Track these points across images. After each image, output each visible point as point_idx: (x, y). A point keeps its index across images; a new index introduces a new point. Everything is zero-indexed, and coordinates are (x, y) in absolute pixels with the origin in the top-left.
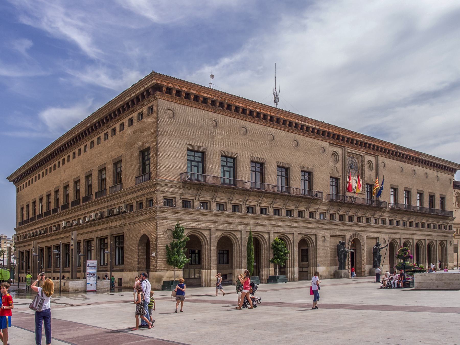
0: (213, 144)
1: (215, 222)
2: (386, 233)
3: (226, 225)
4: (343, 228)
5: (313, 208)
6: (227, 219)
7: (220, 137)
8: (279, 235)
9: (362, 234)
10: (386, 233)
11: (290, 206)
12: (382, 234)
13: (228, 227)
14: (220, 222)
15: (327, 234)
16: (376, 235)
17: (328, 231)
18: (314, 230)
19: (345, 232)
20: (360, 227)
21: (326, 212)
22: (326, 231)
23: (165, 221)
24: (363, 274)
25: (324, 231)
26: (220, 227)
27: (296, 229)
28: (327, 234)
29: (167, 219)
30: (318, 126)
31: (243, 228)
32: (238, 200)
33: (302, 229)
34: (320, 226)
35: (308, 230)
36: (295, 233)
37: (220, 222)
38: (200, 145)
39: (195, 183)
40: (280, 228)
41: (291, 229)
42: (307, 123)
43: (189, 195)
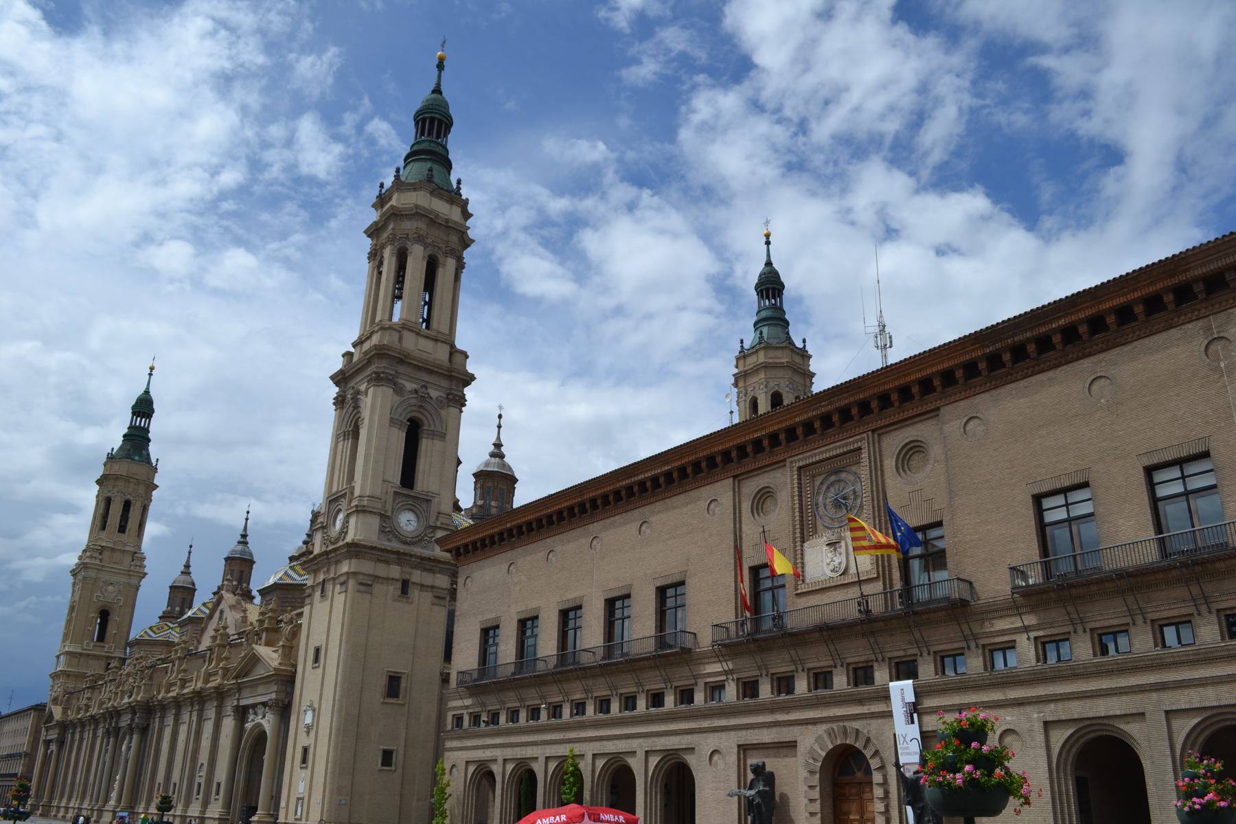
7: (518, 588)
15: (729, 743)
17: (732, 734)
19: (796, 729)
20: (860, 701)
21: (724, 678)
22: (724, 735)
26: (509, 753)
27: (641, 740)
28: (729, 743)
30: (667, 464)
32: (532, 697)
33: (655, 739)
34: (705, 724)
36: (638, 750)
40: (605, 743)
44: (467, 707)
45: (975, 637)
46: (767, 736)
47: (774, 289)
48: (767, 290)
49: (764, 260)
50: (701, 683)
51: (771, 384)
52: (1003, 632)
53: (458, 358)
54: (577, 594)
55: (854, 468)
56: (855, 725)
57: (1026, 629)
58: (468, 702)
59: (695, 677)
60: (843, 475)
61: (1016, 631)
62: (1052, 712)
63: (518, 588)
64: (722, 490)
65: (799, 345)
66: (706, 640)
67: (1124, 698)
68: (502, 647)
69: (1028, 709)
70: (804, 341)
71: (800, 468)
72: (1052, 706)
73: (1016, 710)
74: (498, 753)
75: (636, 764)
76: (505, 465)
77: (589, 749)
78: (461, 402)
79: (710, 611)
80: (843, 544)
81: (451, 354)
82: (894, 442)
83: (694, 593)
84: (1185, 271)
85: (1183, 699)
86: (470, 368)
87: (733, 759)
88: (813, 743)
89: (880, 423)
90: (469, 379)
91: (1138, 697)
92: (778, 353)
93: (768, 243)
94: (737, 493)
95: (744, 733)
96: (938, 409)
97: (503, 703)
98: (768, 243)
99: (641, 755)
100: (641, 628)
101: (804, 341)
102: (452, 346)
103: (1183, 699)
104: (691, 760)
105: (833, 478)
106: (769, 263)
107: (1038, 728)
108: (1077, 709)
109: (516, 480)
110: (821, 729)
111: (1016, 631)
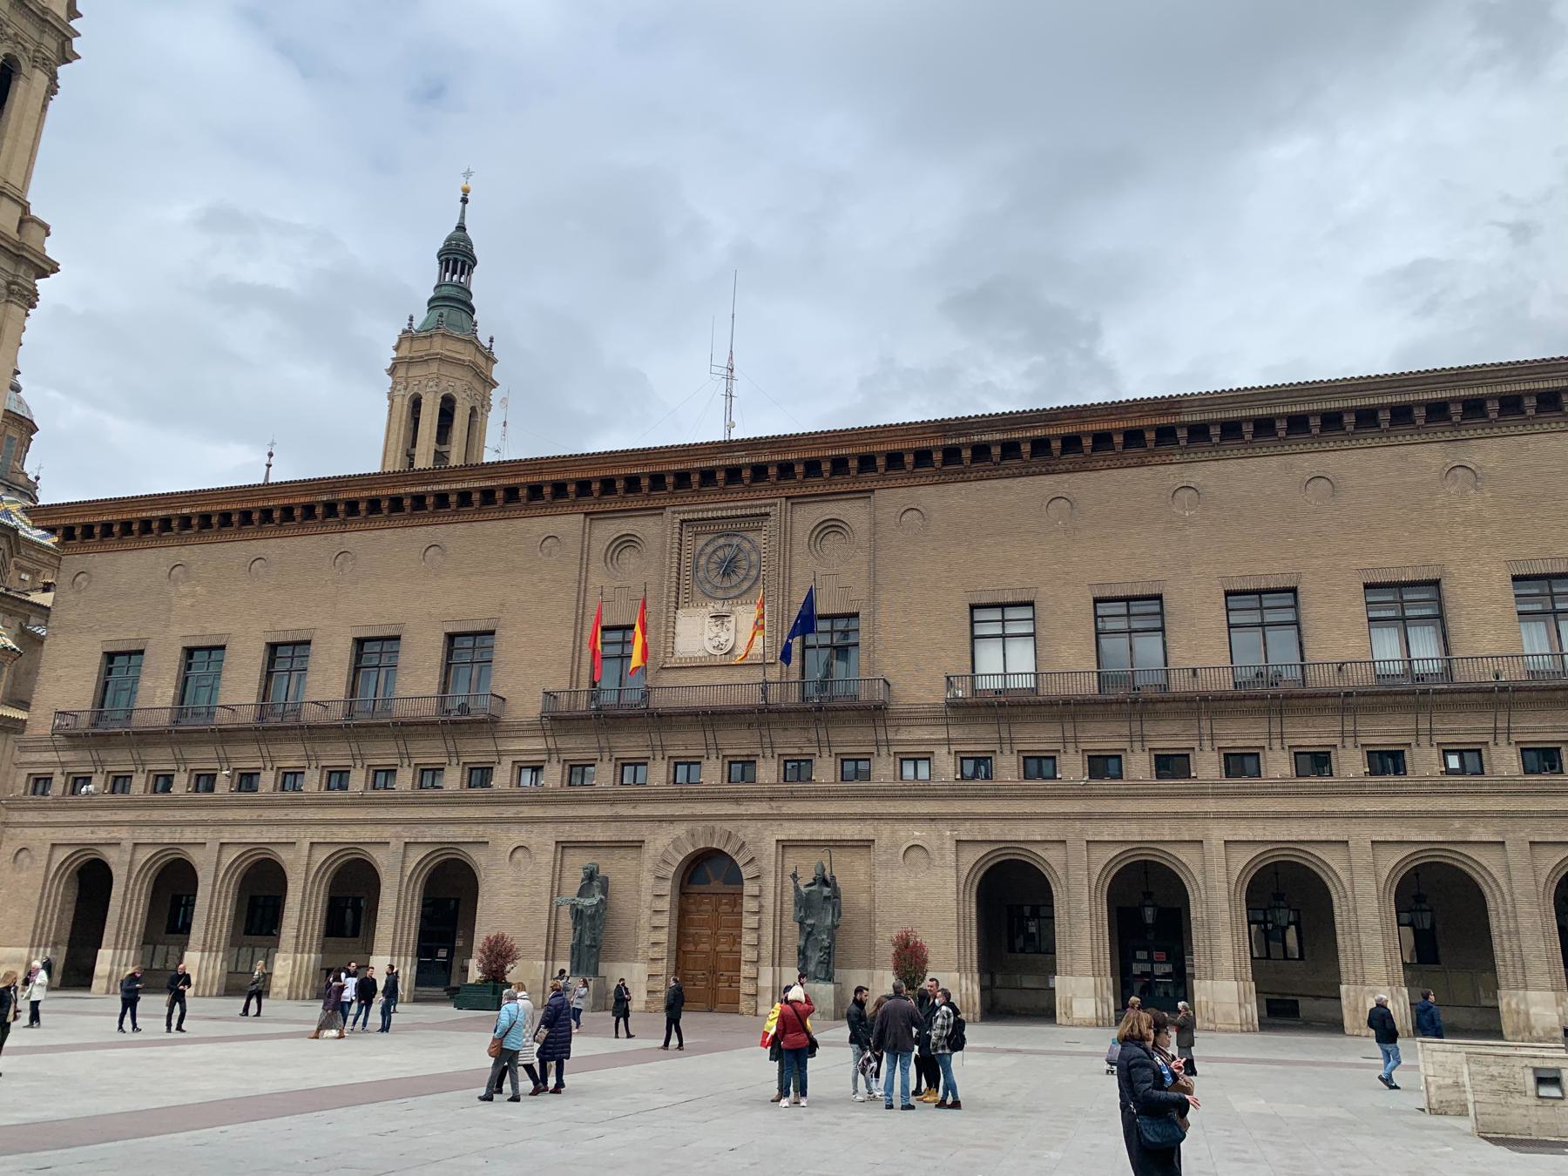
0: (167, 626)
1: (132, 824)
2: (932, 818)
3: (163, 830)
4: (633, 812)
5: (477, 750)
6: (179, 815)
7: (188, 602)
8: (983, 850)
9: (748, 831)
10: (932, 818)
11: (1313, 734)
12: (898, 826)
13: (167, 835)
14: (145, 824)
15: (543, 840)
16: (850, 831)
18: (481, 827)
19: (645, 825)
20: (737, 800)
22: (536, 828)
23: (18, 831)
24: (743, 1006)
25: (525, 827)
27: (399, 828)
28: (543, 840)
29: (23, 825)
31: (209, 835)
33: (422, 828)
35: (451, 828)
36: (393, 841)
37: (145, 824)
38: (133, 636)
39: (104, 730)
40: (335, 829)
41: (380, 828)
42: (446, 482)
43: (79, 761)
44: (63, 764)
45: (888, 743)
46: (600, 833)
47: (464, 263)
48: (456, 261)
49: (456, 222)
50: (507, 762)
51: (444, 384)
52: (921, 742)
53: (33, 232)
54: (303, 624)
55: (751, 535)
56: (729, 826)
57: (949, 741)
58: (67, 756)
59: (499, 753)
60: (735, 541)
61: (938, 742)
62: (966, 831)
63: (188, 602)
64: (567, 524)
65: (484, 339)
66: (526, 706)
67: (1047, 824)
68: (146, 682)
69: (941, 826)
70: (491, 340)
71: (683, 521)
72: (968, 824)
73: (926, 826)
74: (122, 834)
75: (384, 861)
76: (20, 402)
77: (305, 837)
78: (31, 299)
79: (533, 671)
80: (732, 618)
81: (21, 222)
82: (809, 516)
83: (505, 649)
84: (1178, 414)
85: (1107, 832)
86: (52, 248)
87: (546, 858)
88: (668, 844)
89: (797, 492)
90: (47, 268)
91: (1062, 824)
92: (459, 346)
93: (465, 201)
94: (586, 535)
95: (567, 827)
96: (872, 491)
97: (102, 763)
98: (465, 201)
99: (396, 845)
100: (417, 682)
101: (491, 340)
102: (25, 208)
103: (1107, 832)
104: (478, 858)
105: (722, 541)
106: (461, 228)
107: (950, 845)
108: (995, 831)
109: (33, 429)
110: (681, 830)
111: (938, 742)
